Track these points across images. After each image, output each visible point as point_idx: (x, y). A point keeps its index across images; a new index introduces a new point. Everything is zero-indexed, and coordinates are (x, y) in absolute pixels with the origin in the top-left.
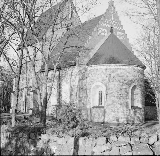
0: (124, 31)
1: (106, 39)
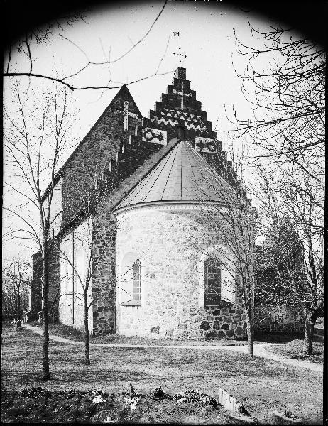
0: (213, 135)
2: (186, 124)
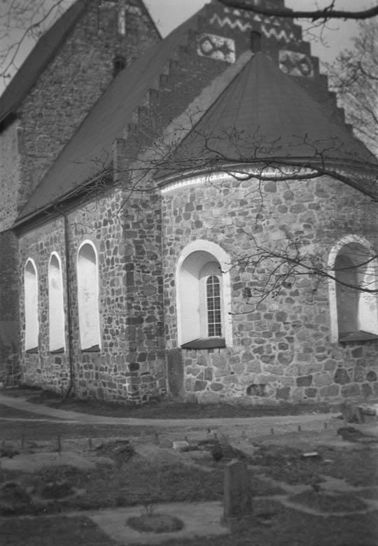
0: (306, 47)
1: (235, 74)
2: (263, 29)
